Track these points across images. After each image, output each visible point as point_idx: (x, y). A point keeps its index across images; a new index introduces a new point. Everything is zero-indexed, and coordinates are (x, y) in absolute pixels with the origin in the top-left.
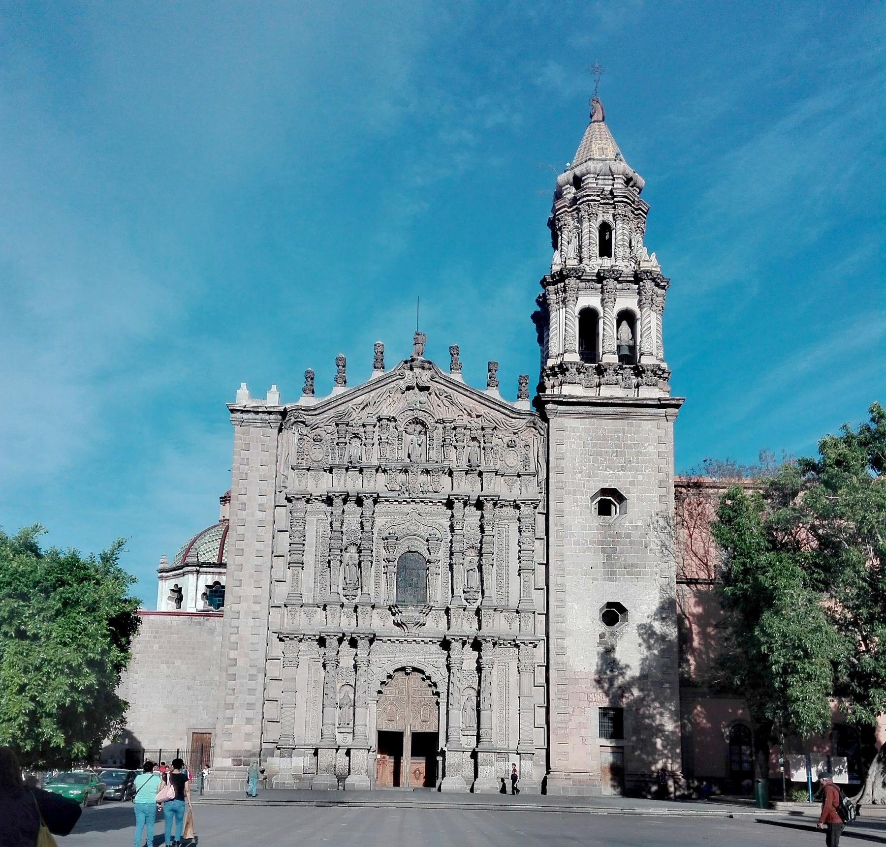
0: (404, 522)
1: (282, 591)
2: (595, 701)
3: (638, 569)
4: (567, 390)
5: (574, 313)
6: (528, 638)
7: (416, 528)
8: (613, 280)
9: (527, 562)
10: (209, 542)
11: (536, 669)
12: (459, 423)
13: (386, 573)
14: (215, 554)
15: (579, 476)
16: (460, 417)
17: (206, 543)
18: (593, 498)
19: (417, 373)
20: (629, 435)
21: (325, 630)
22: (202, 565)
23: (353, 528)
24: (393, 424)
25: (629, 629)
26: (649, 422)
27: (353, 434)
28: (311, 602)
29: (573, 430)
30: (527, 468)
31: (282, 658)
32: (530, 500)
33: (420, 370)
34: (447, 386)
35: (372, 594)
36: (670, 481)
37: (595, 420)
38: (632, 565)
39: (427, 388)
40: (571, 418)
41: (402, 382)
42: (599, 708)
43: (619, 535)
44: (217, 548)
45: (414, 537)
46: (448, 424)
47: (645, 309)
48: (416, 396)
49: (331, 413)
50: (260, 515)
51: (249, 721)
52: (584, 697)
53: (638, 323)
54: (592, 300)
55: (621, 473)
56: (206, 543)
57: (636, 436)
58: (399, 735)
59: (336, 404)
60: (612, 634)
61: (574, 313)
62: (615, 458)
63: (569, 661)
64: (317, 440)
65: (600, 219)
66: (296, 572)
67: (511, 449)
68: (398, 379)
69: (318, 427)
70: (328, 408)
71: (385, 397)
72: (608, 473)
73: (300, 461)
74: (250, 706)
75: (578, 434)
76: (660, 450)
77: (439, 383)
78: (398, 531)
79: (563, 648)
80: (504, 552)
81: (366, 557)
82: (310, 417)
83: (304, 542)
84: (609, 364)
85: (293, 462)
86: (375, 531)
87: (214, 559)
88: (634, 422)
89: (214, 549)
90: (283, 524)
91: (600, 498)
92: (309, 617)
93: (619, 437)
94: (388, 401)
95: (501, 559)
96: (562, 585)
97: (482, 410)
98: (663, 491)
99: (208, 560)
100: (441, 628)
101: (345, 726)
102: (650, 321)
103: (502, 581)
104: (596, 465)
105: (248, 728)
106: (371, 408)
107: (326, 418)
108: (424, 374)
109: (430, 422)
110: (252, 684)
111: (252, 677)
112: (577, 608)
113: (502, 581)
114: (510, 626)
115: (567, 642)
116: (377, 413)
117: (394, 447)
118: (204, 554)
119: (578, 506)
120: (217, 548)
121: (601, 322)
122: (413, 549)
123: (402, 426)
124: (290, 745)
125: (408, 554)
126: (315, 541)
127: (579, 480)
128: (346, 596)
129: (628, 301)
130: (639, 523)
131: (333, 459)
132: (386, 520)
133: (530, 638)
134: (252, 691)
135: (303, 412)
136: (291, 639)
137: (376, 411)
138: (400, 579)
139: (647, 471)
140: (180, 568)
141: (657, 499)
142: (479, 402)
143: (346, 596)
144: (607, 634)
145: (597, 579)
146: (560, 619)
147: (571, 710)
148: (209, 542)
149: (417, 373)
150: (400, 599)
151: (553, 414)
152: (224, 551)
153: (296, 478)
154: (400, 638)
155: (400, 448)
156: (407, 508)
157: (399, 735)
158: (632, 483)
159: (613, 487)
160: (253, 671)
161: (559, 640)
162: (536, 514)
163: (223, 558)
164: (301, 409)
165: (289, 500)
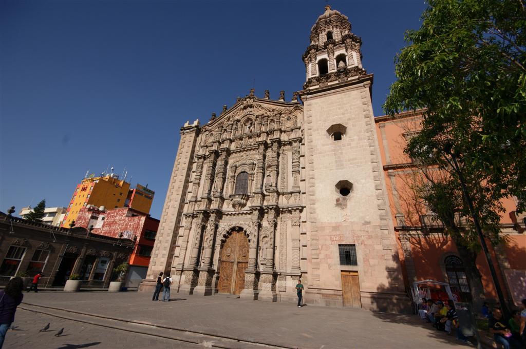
29: (316, 104)
33: (249, 99)
37: (327, 97)
38: (353, 159)
50: (183, 165)
52: (328, 238)
54: (325, 56)
55: (342, 116)
63: (318, 217)
64: (212, 134)
65: (327, 31)
74: (165, 248)
78: (238, 164)
79: (314, 209)
85: (202, 144)
93: (340, 101)
96: (313, 175)
97: (274, 107)
109: (253, 118)
121: (328, 62)
122: (243, 170)
144: (341, 199)
145: (332, 170)
147: (320, 247)
151: (305, 99)
156: (242, 154)
158: (349, 119)
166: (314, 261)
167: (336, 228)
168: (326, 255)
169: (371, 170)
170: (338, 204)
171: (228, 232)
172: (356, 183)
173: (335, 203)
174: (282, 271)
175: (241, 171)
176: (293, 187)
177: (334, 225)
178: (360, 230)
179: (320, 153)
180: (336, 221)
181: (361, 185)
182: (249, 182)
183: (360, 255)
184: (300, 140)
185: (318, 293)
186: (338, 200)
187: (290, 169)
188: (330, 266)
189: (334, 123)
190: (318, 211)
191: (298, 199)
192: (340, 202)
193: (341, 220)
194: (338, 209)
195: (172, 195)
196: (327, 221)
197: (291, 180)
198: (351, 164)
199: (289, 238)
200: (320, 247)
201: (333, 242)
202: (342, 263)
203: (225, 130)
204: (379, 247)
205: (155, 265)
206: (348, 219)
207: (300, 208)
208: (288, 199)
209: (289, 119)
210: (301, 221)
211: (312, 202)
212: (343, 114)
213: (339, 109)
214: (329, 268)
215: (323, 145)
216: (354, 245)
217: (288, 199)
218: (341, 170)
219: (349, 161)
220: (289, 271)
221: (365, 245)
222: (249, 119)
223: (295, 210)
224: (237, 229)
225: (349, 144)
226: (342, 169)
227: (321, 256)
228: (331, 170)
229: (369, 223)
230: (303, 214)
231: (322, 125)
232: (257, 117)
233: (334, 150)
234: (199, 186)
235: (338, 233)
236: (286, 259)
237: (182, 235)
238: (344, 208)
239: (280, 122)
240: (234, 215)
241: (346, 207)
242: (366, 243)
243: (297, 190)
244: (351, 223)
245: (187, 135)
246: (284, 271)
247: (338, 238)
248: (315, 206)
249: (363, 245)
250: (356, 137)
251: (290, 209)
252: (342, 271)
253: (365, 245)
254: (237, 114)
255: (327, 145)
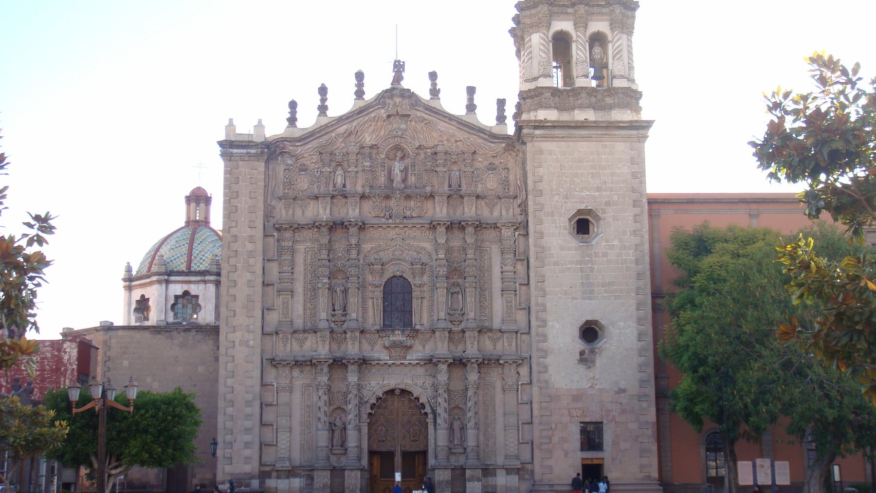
0: (388, 248)
1: (273, 318)
2: (577, 416)
3: (615, 287)
4: (542, 115)
5: (548, 38)
6: (510, 358)
7: (400, 252)
8: (584, 6)
9: (510, 283)
10: (176, 247)
11: (520, 386)
12: (439, 149)
13: (373, 298)
14: (183, 261)
15: (556, 198)
16: (440, 143)
17: (173, 249)
18: (570, 220)
19: (398, 102)
20: (603, 157)
21: (317, 357)
22: (170, 273)
23: (340, 255)
24: (375, 151)
25: (608, 346)
26: (622, 143)
27: (338, 162)
28: (301, 328)
30: (507, 190)
31: (275, 384)
32: (510, 223)
33: (400, 100)
34: (427, 114)
35: (360, 319)
36: (644, 201)
37: (571, 143)
38: (611, 284)
39: (409, 116)
40: (547, 141)
41: (383, 111)
42: (581, 423)
43: (596, 255)
44: (185, 254)
45: (399, 262)
46: (428, 150)
47: (616, 33)
48: (398, 124)
49: (315, 144)
50: (250, 246)
51: (247, 445)
53: (610, 46)
55: (596, 194)
56: (173, 249)
57: (610, 157)
58: (391, 455)
59: (320, 134)
60: (592, 351)
61: (548, 39)
62: (591, 180)
66: (286, 300)
67: (490, 172)
68: (380, 108)
69: (303, 157)
70: (312, 138)
71: (367, 125)
72: (584, 194)
73: (286, 191)
74: (248, 431)
75: (555, 157)
76: (633, 171)
77: (419, 110)
79: (546, 367)
80: (486, 274)
81: (353, 284)
82: (295, 148)
83: (292, 271)
84: (582, 88)
86: (361, 257)
87: (182, 266)
88: (608, 143)
89: (182, 256)
90: (272, 253)
91: (577, 218)
92: (302, 343)
94: (370, 129)
95: (484, 281)
98: (637, 210)
99: (176, 267)
100: (428, 351)
101: (337, 448)
102: (620, 45)
103: (485, 302)
104: (572, 187)
105: (247, 452)
106: (354, 137)
107: (310, 148)
108: (404, 102)
109: (409, 150)
110: (249, 410)
111: (248, 403)
112: (557, 327)
113: (485, 302)
114: (495, 346)
115: (549, 360)
116: (358, 142)
117: (377, 174)
118: (172, 261)
119: (556, 227)
120: (185, 254)
121: (574, 45)
122: (398, 274)
123: (384, 153)
124: (286, 467)
125: (394, 279)
126: (302, 269)
127: (557, 201)
128: (334, 322)
129: (599, 26)
130: (616, 243)
131: (319, 187)
132: (372, 246)
133: (513, 357)
134: (248, 417)
135: (288, 143)
136: (284, 366)
137: (359, 140)
138: (386, 304)
139: (622, 192)
140: (148, 277)
141: (631, 218)
142: (458, 128)
143: (334, 322)
144: (586, 351)
145: (575, 298)
146: (541, 339)
148: (176, 247)
149: (398, 102)
150: (387, 323)
151: (529, 139)
152: (193, 257)
153: (282, 208)
154: (388, 362)
155: (383, 175)
157: (391, 455)
158: (608, 204)
159: (589, 208)
160: (249, 397)
161: (541, 360)
162: (516, 236)
163: (192, 265)
164: (286, 141)
165: (278, 230)
166: (544, 447)
167: (577, 397)
168: (562, 437)
169: (634, 307)
170: (585, 359)
171: (379, 399)
172: (611, 327)
173: (578, 357)
174: (488, 463)
175: (392, 275)
176: (503, 321)
177: (575, 393)
178: (611, 402)
179: (556, 264)
180: (578, 387)
181: (618, 331)
182: (415, 303)
183: (608, 438)
184: (523, 227)
185: (550, 491)
186: (582, 353)
187: (497, 284)
188: (566, 454)
189: (583, 207)
190: (551, 370)
191: (514, 344)
192: (585, 356)
193: (585, 385)
194: (582, 368)
195: (235, 316)
196: (564, 387)
197: (498, 305)
198: (606, 292)
199: (499, 411)
200: (553, 426)
201: (573, 419)
202: (582, 449)
203: (339, 164)
204: (633, 426)
205: (231, 464)
206: (596, 385)
207: (520, 362)
208: (494, 341)
209: (492, 168)
210: (520, 383)
211: (543, 354)
212: (599, 189)
213: (592, 177)
214: (566, 456)
215: (562, 248)
216: (602, 423)
217: (494, 341)
218: (589, 301)
219: (603, 287)
220: (500, 461)
221: (616, 422)
222: (398, 148)
223: (510, 364)
224: (397, 392)
225: (605, 255)
226: (591, 299)
227: (555, 439)
228: (573, 298)
229: (623, 391)
230: (524, 371)
231: (562, 206)
232: (420, 147)
233: (580, 262)
234: (292, 298)
235: (580, 405)
236: (495, 445)
237: (275, 403)
238: (590, 367)
239: (473, 172)
240: (390, 366)
241: (595, 365)
242: (617, 420)
243: (514, 327)
244: (600, 390)
245: (241, 163)
246: (492, 462)
247: (579, 413)
248: (546, 360)
249: (613, 423)
250: (616, 243)
251: (501, 362)
252: (582, 459)
253: (616, 422)
254: (368, 128)
255: (569, 249)
